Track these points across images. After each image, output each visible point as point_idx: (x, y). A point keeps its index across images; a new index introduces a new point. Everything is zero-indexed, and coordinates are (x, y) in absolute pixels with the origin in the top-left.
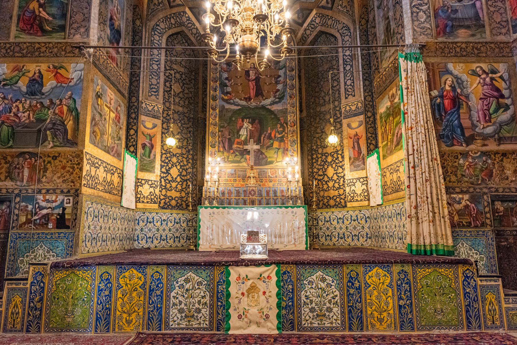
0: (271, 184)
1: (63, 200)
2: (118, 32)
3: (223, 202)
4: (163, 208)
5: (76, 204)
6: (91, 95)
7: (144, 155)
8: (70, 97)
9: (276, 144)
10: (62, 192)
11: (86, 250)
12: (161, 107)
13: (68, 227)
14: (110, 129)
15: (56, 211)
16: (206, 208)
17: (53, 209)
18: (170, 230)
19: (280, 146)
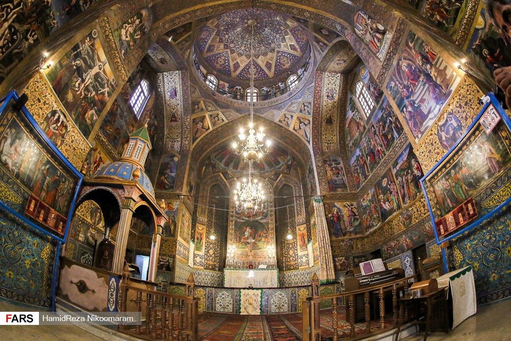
0: (260, 259)
1: (169, 259)
2: (192, 187)
3: (236, 267)
4: (205, 269)
5: (174, 261)
6: (181, 215)
7: (198, 242)
8: (173, 216)
9: (263, 239)
10: (169, 256)
11: (177, 280)
12: (206, 220)
13: (170, 271)
14: (186, 230)
15: (166, 263)
16: (228, 269)
17: (165, 262)
18: (209, 280)
19: (265, 240)
